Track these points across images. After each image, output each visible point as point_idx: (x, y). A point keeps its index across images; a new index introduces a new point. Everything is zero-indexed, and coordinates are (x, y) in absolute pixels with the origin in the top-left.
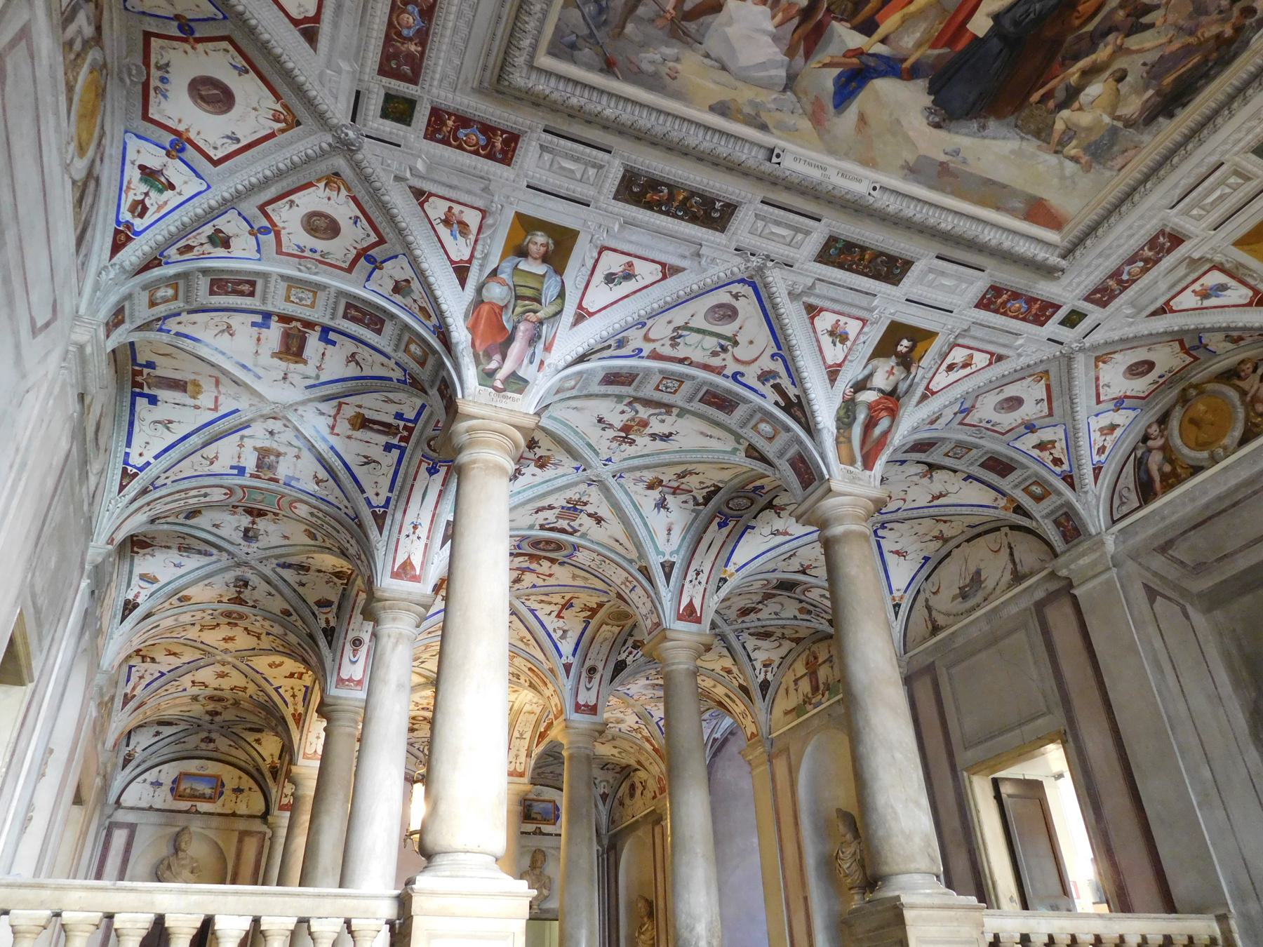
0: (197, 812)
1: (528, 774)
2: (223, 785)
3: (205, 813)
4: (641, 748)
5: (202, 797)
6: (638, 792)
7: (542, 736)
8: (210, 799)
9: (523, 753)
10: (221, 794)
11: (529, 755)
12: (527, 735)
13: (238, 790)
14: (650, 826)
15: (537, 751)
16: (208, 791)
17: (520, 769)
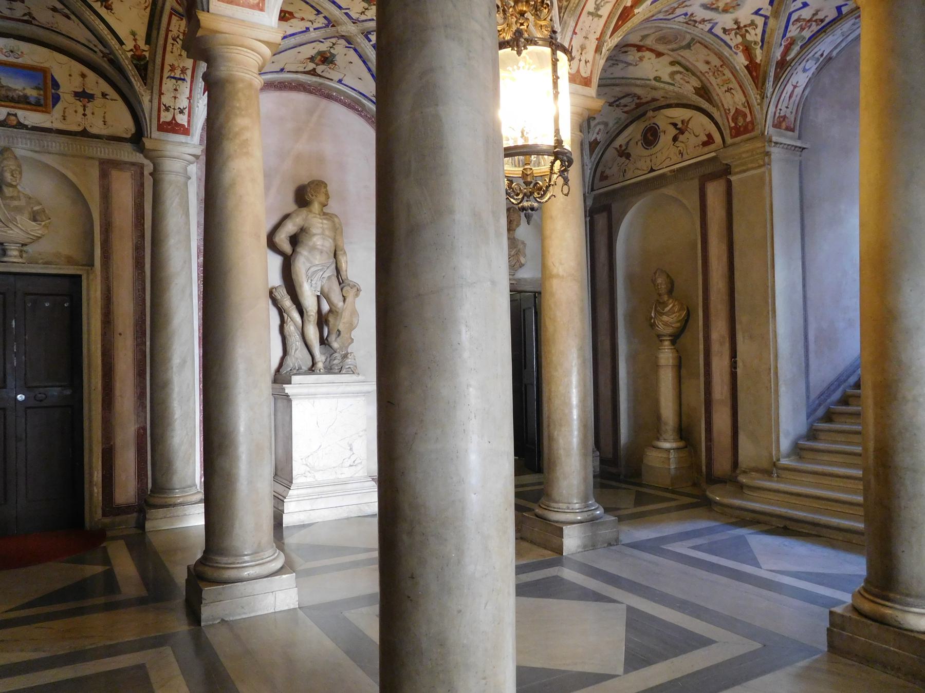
0: (20, 126)
1: (595, 81)
2: (56, 85)
3: (35, 129)
4: (725, 62)
5: (23, 102)
6: (665, 139)
7: (626, 15)
8: (37, 106)
9: (592, 45)
10: (56, 99)
11: (598, 50)
12: (605, 11)
13: (83, 96)
14: (696, 183)
15: (611, 43)
16: (32, 93)
17: (585, 73)
